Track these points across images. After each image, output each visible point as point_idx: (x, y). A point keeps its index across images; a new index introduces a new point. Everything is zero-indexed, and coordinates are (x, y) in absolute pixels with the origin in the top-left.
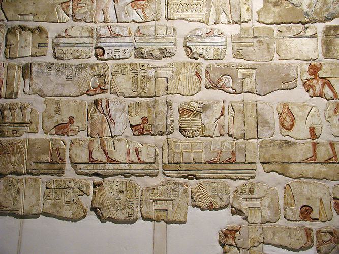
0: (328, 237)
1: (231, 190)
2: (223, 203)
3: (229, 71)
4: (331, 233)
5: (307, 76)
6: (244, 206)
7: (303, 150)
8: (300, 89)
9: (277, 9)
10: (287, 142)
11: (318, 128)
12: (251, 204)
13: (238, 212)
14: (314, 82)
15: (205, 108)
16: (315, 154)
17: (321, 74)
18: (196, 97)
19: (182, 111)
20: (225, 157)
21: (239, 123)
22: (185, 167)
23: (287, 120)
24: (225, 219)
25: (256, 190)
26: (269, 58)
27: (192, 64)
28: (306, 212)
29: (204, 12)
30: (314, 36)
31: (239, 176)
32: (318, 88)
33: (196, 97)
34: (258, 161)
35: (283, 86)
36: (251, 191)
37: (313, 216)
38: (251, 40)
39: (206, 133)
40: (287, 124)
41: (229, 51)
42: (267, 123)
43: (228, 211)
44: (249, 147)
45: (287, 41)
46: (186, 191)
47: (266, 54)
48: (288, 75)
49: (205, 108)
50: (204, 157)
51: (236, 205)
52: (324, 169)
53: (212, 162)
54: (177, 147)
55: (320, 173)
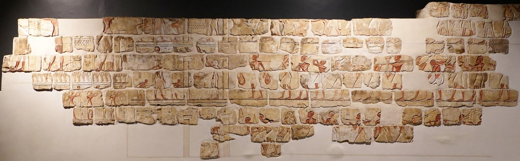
0: (256, 130)
1: (216, 111)
2: (213, 117)
3: (216, 58)
4: (257, 128)
5: (252, 60)
6: (221, 119)
7: (248, 94)
8: (249, 67)
9: (240, 28)
10: (241, 91)
11: (255, 84)
12: (224, 117)
13: (219, 120)
14: (255, 63)
15: (205, 75)
16: (253, 96)
17: (258, 59)
18: (202, 70)
19: (195, 77)
20: (214, 97)
21: (220, 82)
22: (196, 101)
23: (242, 80)
24: (213, 123)
25: (227, 111)
26: (235, 52)
27: (200, 55)
28: (248, 120)
29: (205, 30)
30: (256, 41)
31: (220, 105)
32: (256, 66)
33: (202, 70)
34: (228, 98)
35: (241, 65)
36: (225, 111)
37: (250, 121)
38: (227, 44)
39: (206, 87)
40: (241, 82)
41: (217, 48)
42: (233, 82)
43: (214, 120)
44: (225, 93)
45: (244, 44)
46: (197, 111)
47: (234, 50)
48: (243, 60)
49: (205, 75)
50: (205, 97)
51: (218, 117)
52: (256, 102)
53: (208, 99)
54: (193, 93)
55: (255, 103)
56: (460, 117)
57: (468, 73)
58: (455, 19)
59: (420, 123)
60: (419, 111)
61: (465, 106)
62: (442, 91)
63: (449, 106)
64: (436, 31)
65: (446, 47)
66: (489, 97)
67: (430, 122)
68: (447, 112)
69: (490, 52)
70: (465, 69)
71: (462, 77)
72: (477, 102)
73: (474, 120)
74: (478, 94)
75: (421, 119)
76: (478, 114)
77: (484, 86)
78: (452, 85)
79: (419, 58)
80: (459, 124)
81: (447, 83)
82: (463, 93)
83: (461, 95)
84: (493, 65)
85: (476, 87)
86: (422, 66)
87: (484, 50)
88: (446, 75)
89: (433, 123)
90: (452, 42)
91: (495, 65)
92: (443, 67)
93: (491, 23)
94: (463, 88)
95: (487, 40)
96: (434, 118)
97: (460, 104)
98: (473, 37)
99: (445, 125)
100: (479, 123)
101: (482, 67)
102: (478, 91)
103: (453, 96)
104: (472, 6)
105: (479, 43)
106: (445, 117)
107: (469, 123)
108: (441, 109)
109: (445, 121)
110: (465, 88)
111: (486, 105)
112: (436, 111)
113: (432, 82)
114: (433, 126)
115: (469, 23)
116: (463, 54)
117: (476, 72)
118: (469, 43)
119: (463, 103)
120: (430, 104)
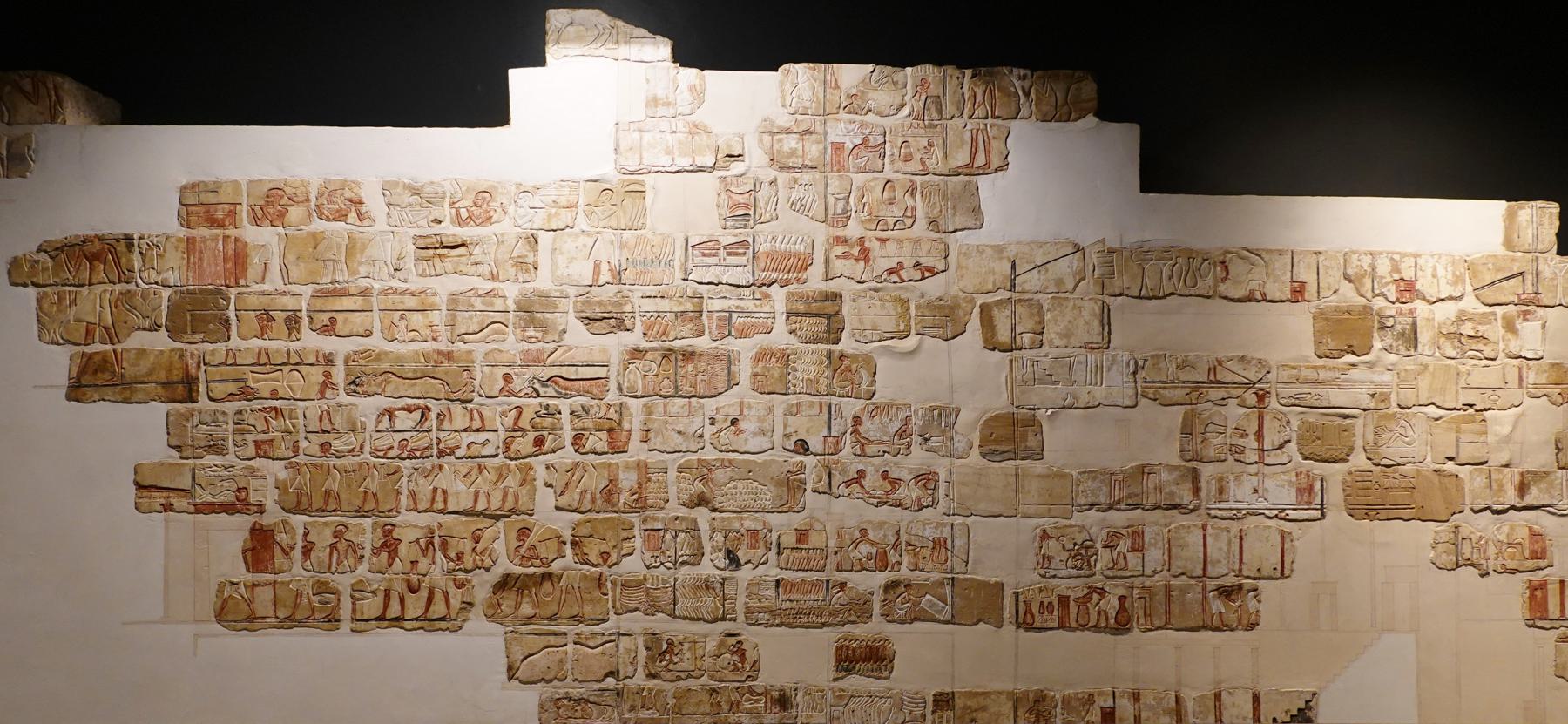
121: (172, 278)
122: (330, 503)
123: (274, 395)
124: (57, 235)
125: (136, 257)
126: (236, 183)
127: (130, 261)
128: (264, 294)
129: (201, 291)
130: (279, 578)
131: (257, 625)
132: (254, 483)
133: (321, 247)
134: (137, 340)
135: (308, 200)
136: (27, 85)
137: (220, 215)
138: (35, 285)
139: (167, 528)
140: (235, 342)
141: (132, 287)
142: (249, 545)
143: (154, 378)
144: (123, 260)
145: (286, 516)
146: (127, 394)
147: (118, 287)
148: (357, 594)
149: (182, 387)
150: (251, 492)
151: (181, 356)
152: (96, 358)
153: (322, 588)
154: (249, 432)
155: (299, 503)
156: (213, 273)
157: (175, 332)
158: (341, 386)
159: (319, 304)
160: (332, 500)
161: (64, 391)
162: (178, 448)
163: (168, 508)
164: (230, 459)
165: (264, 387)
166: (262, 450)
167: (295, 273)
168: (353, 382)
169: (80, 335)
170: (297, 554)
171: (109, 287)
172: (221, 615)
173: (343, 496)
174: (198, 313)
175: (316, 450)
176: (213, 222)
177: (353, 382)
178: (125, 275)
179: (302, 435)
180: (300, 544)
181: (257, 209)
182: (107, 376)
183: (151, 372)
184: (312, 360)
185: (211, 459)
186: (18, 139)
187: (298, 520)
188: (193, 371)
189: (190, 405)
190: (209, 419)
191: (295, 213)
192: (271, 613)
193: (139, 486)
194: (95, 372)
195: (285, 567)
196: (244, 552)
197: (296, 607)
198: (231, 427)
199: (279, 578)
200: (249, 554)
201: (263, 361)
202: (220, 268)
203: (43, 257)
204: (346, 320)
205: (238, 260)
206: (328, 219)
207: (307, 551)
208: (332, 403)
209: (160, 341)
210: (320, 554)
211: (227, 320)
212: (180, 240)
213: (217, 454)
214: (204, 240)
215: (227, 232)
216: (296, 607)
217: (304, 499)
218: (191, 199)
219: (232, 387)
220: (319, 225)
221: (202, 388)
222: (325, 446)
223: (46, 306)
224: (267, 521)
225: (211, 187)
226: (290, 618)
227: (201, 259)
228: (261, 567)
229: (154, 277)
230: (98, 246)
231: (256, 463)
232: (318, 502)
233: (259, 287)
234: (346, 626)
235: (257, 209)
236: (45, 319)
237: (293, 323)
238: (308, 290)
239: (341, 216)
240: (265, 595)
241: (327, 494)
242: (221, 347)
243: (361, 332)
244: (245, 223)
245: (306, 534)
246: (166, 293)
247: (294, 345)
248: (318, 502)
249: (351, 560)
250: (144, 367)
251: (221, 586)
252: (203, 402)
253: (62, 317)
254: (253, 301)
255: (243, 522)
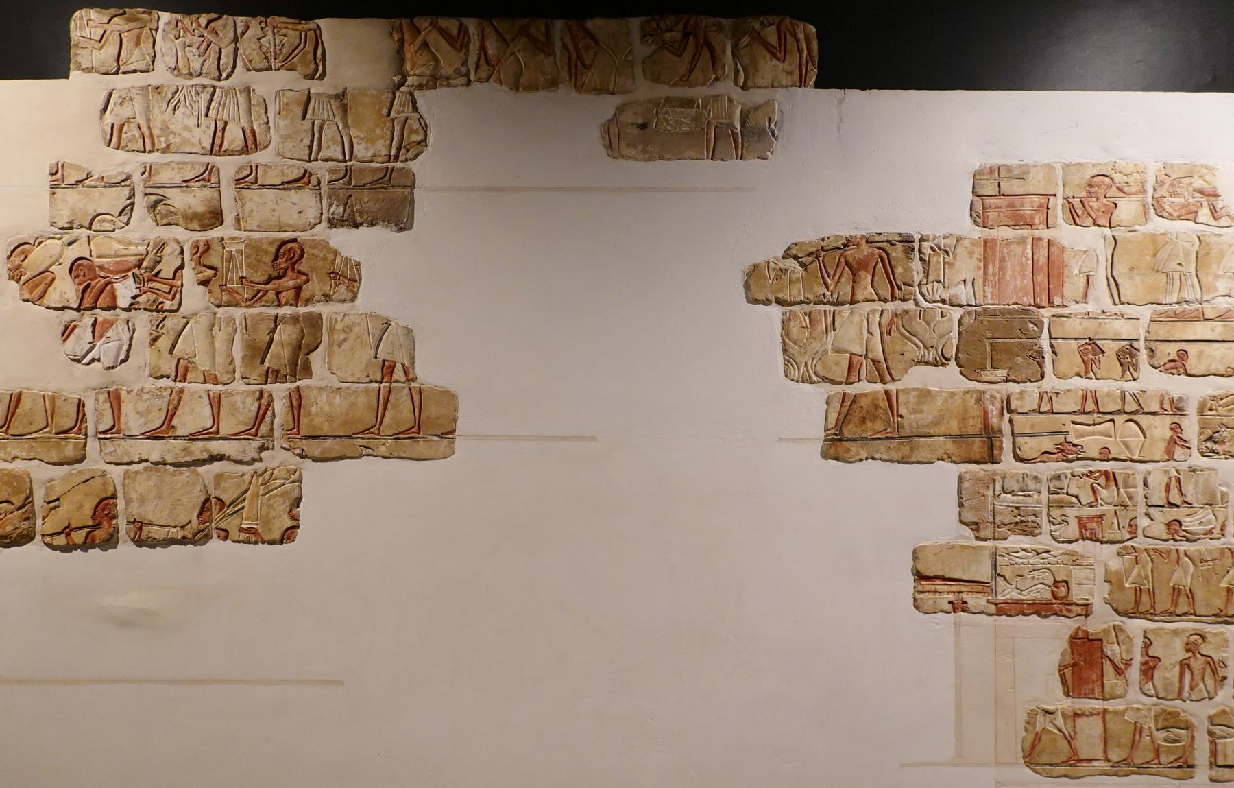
56: (205, 506)
57: (238, 313)
58: (181, 82)
59: (24, 538)
60: (21, 484)
61: (221, 458)
62: (123, 394)
63: (154, 458)
64: (95, 130)
65: (141, 203)
66: (330, 418)
67: (67, 530)
68: (142, 485)
69: (333, 224)
70: (225, 297)
71: (210, 328)
72: (279, 442)
73: (267, 523)
74: (280, 406)
75: (29, 517)
76: (284, 494)
77: (307, 371)
78: (168, 366)
79: (20, 249)
80: (199, 538)
81: (142, 356)
82: (216, 403)
83: (207, 411)
84: (345, 278)
85: (274, 375)
86: (37, 287)
87: (300, 212)
88: (143, 322)
89: (78, 537)
90: (164, 177)
91: (355, 281)
92: (125, 291)
93: (341, 97)
94: (216, 381)
95: (321, 170)
96: (85, 516)
97: (199, 449)
98: (256, 158)
99: (140, 543)
100: (288, 535)
101: (298, 289)
102: (279, 391)
103: (171, 415)
104: (254, 23)
105: (286, 185)
106: (136, 511)
107: (243, 536)
108: (116, 473)
109: (138, 525)
110: (224, 378)
111: (317, 453)
112: (97, 482)
113: (79, 353)
114: (86, 546)
115: (242, 99)
116: (215, 233)
117: (272, 311)
118: (246, 181)
119: (216, 446)
120: (70, 451)
121: (964, 294)
122: (1181, 601)
123: (1105, 454)
124: (809, 235)
125: (916, 265)
126: (1049, 167)
127: (908, 270)
128: (1088, 316)
129: (1002, 313)
130: (1110, 705)
131: (1082, 768)
132: (1078, 574)
133: (1162, 254)
134: (916, 378)
135: (1144, 191)
136: (771, 35)
137: (1027, 210)
138: (779, 302)
139: (957, 634)
140: (1050, 382)
141: (910, 305)
142: (1068, 660)
143: (942, 430)
144: (899, 270)
145: (1119, 620)
146: (906, 450)
147: (891, 306)
148: (1218, 730)
149: (981, 443)
150: (1074, 588)
151: (979, 400)
152: (864, 402)
153: (1170, 721)
154: (1071, 505)
155: (1137, 603)
156: (1018, 288)
157: (970, 368)
158: (1194, 443)
159: (1162, 331)
160: (1183, 600)
161: (819, 446)
162: (975, 525)
163: (959, 606)
164: (1044, 541)
165: (1091, 442)
166: (1088, 530)
167: (1127, 291)
168: (1210, 439)
169: (840, 372)
170: (1134, 673)
171: (878, 306)
172: (1031, 756)
173: (1199, 594)
174: (1000, 342)
175: (1160, 530)
176: (1018, 220)
177: (1210, 439)
178: (897, 289)
179: (1142, 509)
180: (1138, 659)
181: (1076, 202)
182: (879, 426)
183: (937, 422)
184: (1155, 407)
185: (1017, 541)
186: (757, 108)
187: (1136, 626)
188: (994, 421)
189: (989, 467)
190: (1016, 487)
191: (1127, 209)
192: (1100, 755)
193: (920, 576)
194: (863, 420)
195: (1119, 691)
196: (1062, 668)
197: (1133, 745)
198: (1044, 496)
199: (1110, 705)
200: (1068, 672)
201: (1091, 406)
202: (1028, 281)
203: (792, 264)
204: (1201, 354)
205: (1052, 269)
206: (1170, 217)
207: (1148, 670)
208: (1183, 466)
209: (949, 379)
210: (1167, 673)
211: (1040, 353)
212: (974, 243)
213: (1026, 533)
214: (1008, 243)
215: (1037, 233)
216: (1133, 745)
217: (1145, 598)
218: (991, 189)
219: (1048, 444)
220: (1158, 225)
221: (1007, 444)
222: (1174, 525)
223: (794, 330)
224: (1094, 626)
225: (1016, 172)
226: (1126, 762)
227: (1002, 268)
228: (1086, 689)
229: (940, 293)
230: (866, 249)
231: (1080, 547)
232: (1163, 602)
233: (1080, 308)
234: (1202, 774)
235: (1076, 202)
236: (794, 349)
237: (1127, 359)
238: (1146, 313)
239: (1190, 214)
240: (1090, 731)
241: (1176, 591)
242: (1033, 388)
243: (1222, 370)
244: (1060, 221)
245: (1148, 645)
246: (956, 313)
247: (1131, 387)
248: (1163, 602)
249: (1210, 683)
250: (929, 412)
251: (1032, 714)
252: (1008, 463)
253: (816, 345)
254: (1075, 327)
255: (1058, 629)
